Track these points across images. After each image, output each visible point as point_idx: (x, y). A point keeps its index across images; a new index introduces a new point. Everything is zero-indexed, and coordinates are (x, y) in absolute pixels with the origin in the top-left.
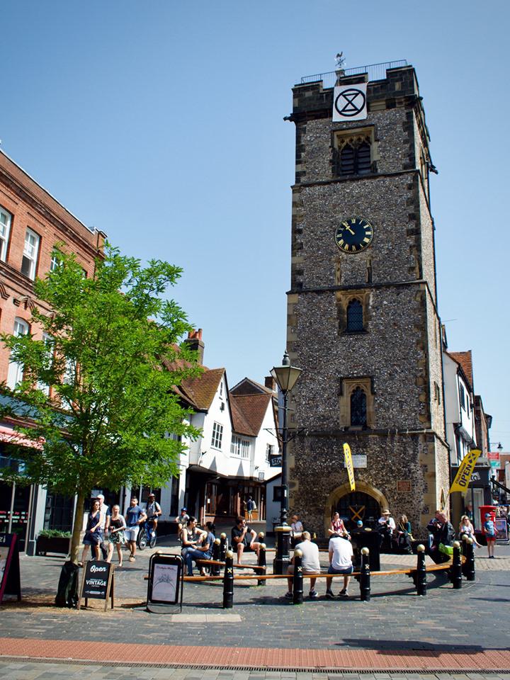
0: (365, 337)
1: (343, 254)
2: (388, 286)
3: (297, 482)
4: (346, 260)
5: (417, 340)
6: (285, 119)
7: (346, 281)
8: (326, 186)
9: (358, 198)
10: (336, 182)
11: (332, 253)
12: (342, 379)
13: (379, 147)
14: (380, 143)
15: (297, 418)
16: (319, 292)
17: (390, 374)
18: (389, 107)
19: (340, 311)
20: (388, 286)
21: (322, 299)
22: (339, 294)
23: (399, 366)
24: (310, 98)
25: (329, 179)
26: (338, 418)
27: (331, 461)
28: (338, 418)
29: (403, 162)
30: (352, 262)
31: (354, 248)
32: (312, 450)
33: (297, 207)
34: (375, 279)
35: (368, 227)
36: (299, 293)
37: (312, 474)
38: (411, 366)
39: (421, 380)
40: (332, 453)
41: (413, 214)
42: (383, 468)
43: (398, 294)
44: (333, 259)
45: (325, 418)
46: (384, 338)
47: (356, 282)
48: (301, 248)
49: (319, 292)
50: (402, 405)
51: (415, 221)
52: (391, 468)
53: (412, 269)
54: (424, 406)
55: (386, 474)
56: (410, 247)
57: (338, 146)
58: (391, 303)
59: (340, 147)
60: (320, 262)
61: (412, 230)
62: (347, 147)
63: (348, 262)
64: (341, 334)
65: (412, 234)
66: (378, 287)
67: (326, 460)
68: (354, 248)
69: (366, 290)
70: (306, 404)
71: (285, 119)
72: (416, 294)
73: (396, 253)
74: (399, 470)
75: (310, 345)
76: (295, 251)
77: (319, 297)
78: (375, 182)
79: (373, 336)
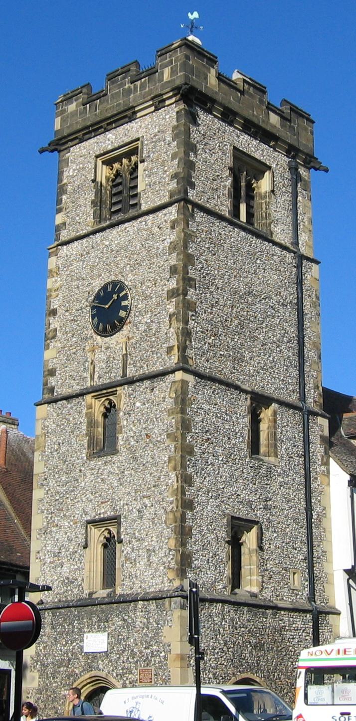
0: (115, 458)
1: (99, 337)
2: (142, 379)
4: (101, 347)
5: (169, 458)
6: (42, 151)
7: (100, 378)
8: (84, 241)
9: (118, 251)
10: (94, 233)
11: (86, 339)
12: (89, 522)
13: (145, 170)
14: (146, 163)
16: (68, 398)
17: (139, 511)
18: (157, 109)
19: (91, 424)
20: (142, 379)
21: (72, 408)
22: (89, 398)
23: (149, 497)
24: (74, 114)
25: (90, 229)
26: (83, 580)
27: (72, 643)
28: (83, 580)
29: (170, 187)
30: (107, 348)
31: (108, 327)
32: (53, 628)
33: (53, 277)
34: (131, 372)
35: (126, 294)
36: (49, 403)
37: (53, 663)
38: (162, 496)
39: (171, 516)
40: (73, 632)
41: (174, 265)
42: (123, 651)
43: (153, 389)
44: (87, 348)
45: (70, 582)
46: (135, 459)
47: (110, 378)
48: (54, 337)
49: (68, 398)
50: (150, 556)
51: (177, 276)
52: (132, 650)
53: (170, 349)
54: (173, 555)
55: (128, 658)
56: (171, 316)
57: (106, 177)
58: (144, 404)
59: (107, 179)
60: (74, 353)
61: (173, 288)
62: (118, 174)
63: (103, 349)
64: (90, 457)
65: (172, 297)
66: (131, 382)
67: (67, 643)
68: (108, 327)
69: (118, 388)
70: (51, 563)
71: (42, 151)
72: (171, 388)
73: (154, 327)
74: (141, 652)
75: (57, 476)
76: (48, 341)
77: (69, 406)
78: (135, 223)
79: (122, 456)
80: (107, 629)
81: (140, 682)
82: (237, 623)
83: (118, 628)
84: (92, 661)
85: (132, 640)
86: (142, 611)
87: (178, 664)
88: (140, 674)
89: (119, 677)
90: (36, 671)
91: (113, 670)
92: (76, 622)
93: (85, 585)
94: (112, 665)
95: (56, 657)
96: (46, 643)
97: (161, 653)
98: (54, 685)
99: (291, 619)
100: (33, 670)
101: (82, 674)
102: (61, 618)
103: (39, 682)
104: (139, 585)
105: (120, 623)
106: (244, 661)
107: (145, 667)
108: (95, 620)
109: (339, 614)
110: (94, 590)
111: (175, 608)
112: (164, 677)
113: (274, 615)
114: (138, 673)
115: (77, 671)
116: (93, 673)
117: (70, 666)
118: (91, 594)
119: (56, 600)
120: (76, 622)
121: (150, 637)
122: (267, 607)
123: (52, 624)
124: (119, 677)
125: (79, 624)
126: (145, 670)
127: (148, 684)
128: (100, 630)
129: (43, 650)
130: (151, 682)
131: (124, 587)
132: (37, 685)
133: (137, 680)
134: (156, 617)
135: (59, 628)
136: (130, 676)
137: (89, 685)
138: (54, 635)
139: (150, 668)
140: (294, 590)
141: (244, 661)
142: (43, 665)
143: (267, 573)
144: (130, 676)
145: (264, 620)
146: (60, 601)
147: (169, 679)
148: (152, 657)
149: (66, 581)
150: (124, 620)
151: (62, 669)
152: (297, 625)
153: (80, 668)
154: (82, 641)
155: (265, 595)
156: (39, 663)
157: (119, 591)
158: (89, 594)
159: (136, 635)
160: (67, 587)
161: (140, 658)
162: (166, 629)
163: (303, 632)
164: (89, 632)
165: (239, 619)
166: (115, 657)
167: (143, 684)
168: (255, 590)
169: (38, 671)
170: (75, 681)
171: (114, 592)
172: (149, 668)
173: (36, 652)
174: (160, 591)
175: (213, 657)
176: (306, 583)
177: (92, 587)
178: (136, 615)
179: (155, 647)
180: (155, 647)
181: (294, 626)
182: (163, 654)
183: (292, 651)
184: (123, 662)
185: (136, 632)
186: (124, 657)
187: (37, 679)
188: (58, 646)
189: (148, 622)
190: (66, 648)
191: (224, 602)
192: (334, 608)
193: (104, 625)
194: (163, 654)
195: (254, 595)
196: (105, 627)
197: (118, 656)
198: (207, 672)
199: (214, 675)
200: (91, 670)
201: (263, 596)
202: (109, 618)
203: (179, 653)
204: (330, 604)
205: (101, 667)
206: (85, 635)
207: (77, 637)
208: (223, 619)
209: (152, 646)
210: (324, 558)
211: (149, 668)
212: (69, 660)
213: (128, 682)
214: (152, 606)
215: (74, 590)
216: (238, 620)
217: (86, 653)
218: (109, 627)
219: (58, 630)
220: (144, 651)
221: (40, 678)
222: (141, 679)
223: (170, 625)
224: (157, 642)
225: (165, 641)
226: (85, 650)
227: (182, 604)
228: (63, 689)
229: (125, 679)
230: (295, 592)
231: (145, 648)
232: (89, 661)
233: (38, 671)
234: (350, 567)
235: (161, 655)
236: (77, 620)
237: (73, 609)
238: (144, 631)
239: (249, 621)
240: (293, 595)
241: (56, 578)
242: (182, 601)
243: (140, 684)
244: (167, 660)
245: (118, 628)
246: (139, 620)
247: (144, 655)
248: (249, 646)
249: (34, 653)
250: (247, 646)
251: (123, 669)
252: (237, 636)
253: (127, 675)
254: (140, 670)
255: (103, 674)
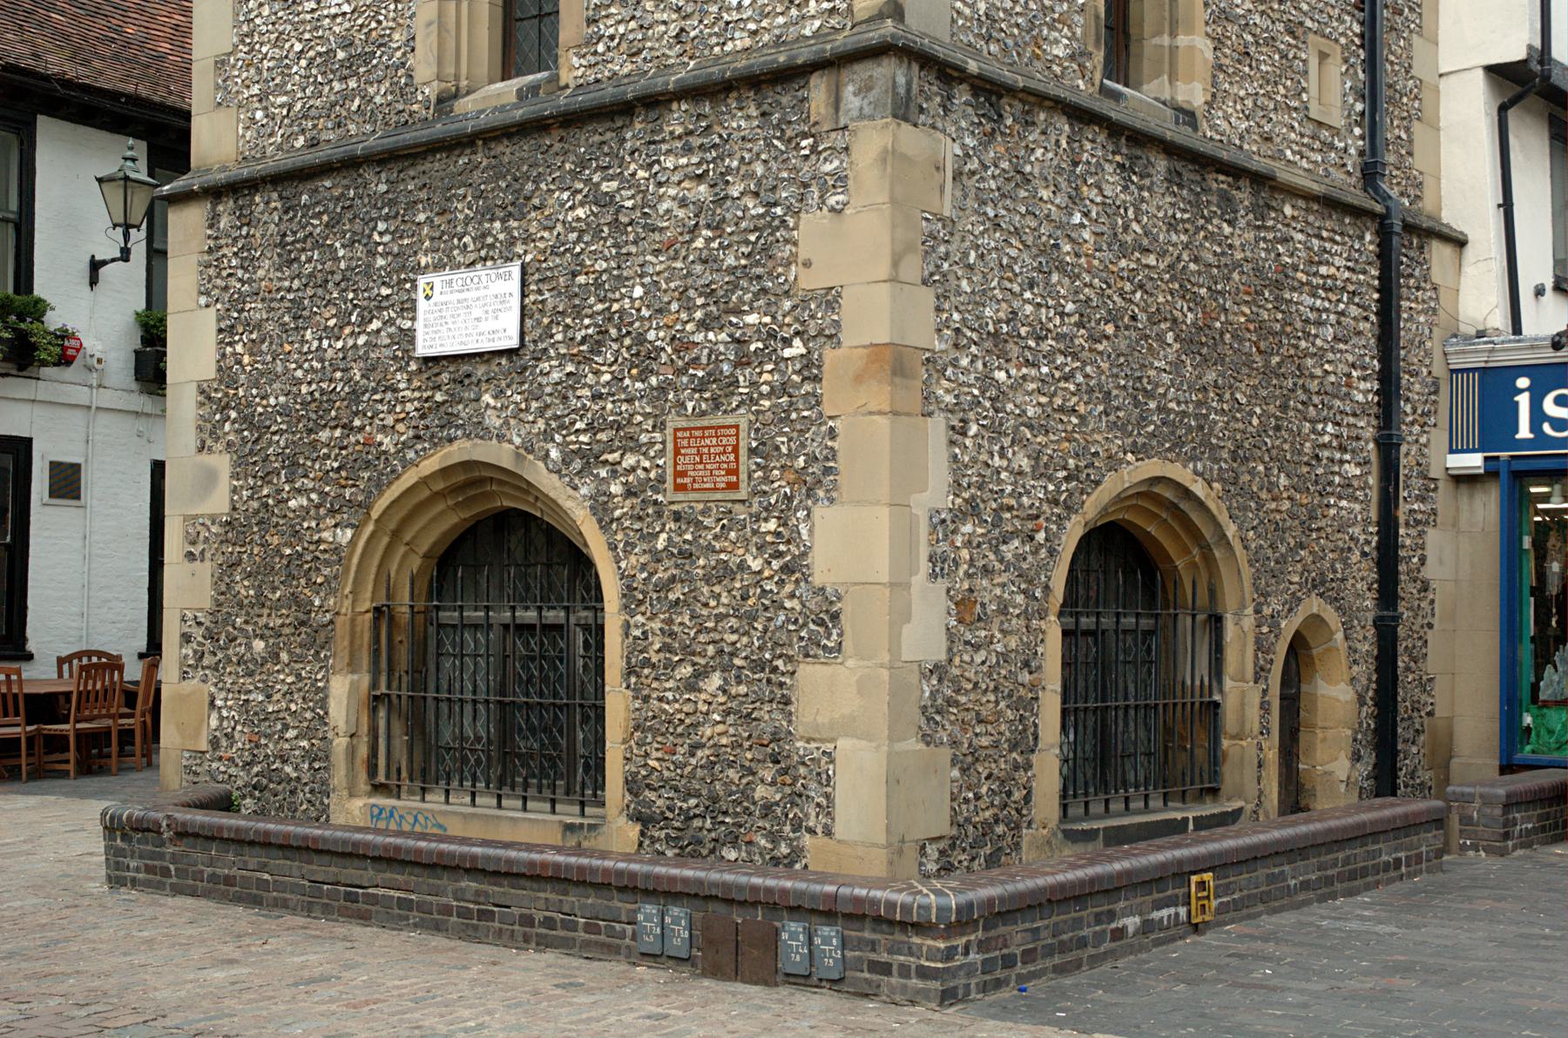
3: (222, 463)
15: (239, 76)
27: (364, 322)
37: (285, 411)
42: (597, 346)
52: (641, 339)
74: (681, 344)
80: (519, 249)
81: (679, 488)
82: (1126, 228)
83: (573, 236)
84: (454, 399)
85: (638, 292)
86: (688, 150)
87: (878, 395)
88: (677, 452)
89: (577, 464)
90: (219, 446)
91: (547, 435)
92: (381, 226)
93: (424, 67)
94: (541, 412)
95: (299, 382)
96: (259, 326)
97: (787, 342)
98: (292, 504)
99: (1315, 242)
100: (209, 442)
101: (411, 455)
102: (318, 215)
103: (234, 490)
104: (673, 29)
105: (580, 212)
106: (1152, 405)
107: (703, 414)
108: (462, 210)
109: (1460, 243)
110: (464, 83)
111: (861, 117)
112: (801, 461)
113: (1260, 211)
114: (670, 446)
115: (387, 442)
116: (461, 450)
117: (357, 423)
118: (444, 101)
119: (300, 142)
120: (381, 226)
121: (731, 270)
122: (1236, 172)
123: (283, 245)
124: (577, 464)
125: (397, 235)
126: (704, 428)
127: (719, 496)
128: (488, 254)
129: (246, 359)
130: (733, 486)
131: (601, 48)
132: (226, 508)
133: (661, 480)
134: (759, 169)
135: (309, 260)
136: (630, 460)
137: (441, 506)
138: (289, 290)
139: (730, 420)
140: (1320, 124)
141: (1152, 405)
142: (247, 420)
143: (1232, 29)
144: (630, 460)
145: (1227, 230)
146: (313, 144)
147: (828, 471)
148: (738, 364)
149: (341, 55)
150: (605, 201)
151: (324, 435)
152: (1333, 270)
153: (401, 427)
154: (409, 308)
155: (1224, 125)
156: (233, 414)
157: (573, 68)
158: (440, 101)
159: (658, 263)
160: (344, 79)
161: (680, 372)
162: (811, 229)
163: (1350, 302)
164: (438, 267)
165: (1137, 210)
166: (556, 376)
167: (692, 496)
168: (1194, 94)
169: (229, 444)
170: (379, 486)
171: (555, 79)
172: (719, 419)
173: (220, 369)
174: (778, 42)
175: (1033, 372)
176: (1359, 107)
177: (450, 70)
178: (656, 168)
179: (752, 319)
180: (752, 319)
181: (1323, 270)
182: (797, 348)
183: (1313, 377)
184: (597, 397)
185: (656, 252)
186: (597, 373)
187: (224, 483)
188: (308, 335)
189: (720, 201)
190: (339, 344)
191: (1080, 115)
192: (1438, 220)
193: (505, 229)
194: (797, 348)
195: (1188, 116)
196: (512, 242)
197: (570, 368)
198: (1006, 442)
199: (1036, 457)
200: (451, 440)
201: (1213, 127)
202: (528, 199)
203: (883, 338)
204: (1427, 204)
205: (493, 421)
206: (422, 281)
207: (385, 291)
208: (1075, 199)
209: (739, 312)
210: (1412, 17)
211: (719, 419)
212: (355, 394)
213: (616, 488)
214: (741, 119)
215: (371, 90)
216: (1131, 213)
217: (427, 360)
218: (528, 239)
219: (309, 268)
220: (699, 338)
221: (235, 476)
222: (683, 474)
223: (832, 201)
224: (764, 291)
225: (810, 281)
226: (423, 348)
227: (902, 91)
228: (330, 522)
229: (603, 473)
230: (1325, 134)
231: (704, 325)
232: (439, 397)
233: (229, 444)
234: (1519, 54)
235: (787, 353)
236: (387, 218)
237: (369, 174)
238: (699, 243)
239: (1172, 224)
240: (1317, 145)
241: (298, 47)
242: (901, 80)
243: (680, 496)
244: (816, 379)
245: (573, 236)
246: (672, 192)
247: (698, 358)
248: (1170, 337)
249: (211, 373)
250: (1160, 338)
251: (591, 428)
252: (1128, 287)
253: (616, 456)
254: (676, 430)
255: (499, 454)
